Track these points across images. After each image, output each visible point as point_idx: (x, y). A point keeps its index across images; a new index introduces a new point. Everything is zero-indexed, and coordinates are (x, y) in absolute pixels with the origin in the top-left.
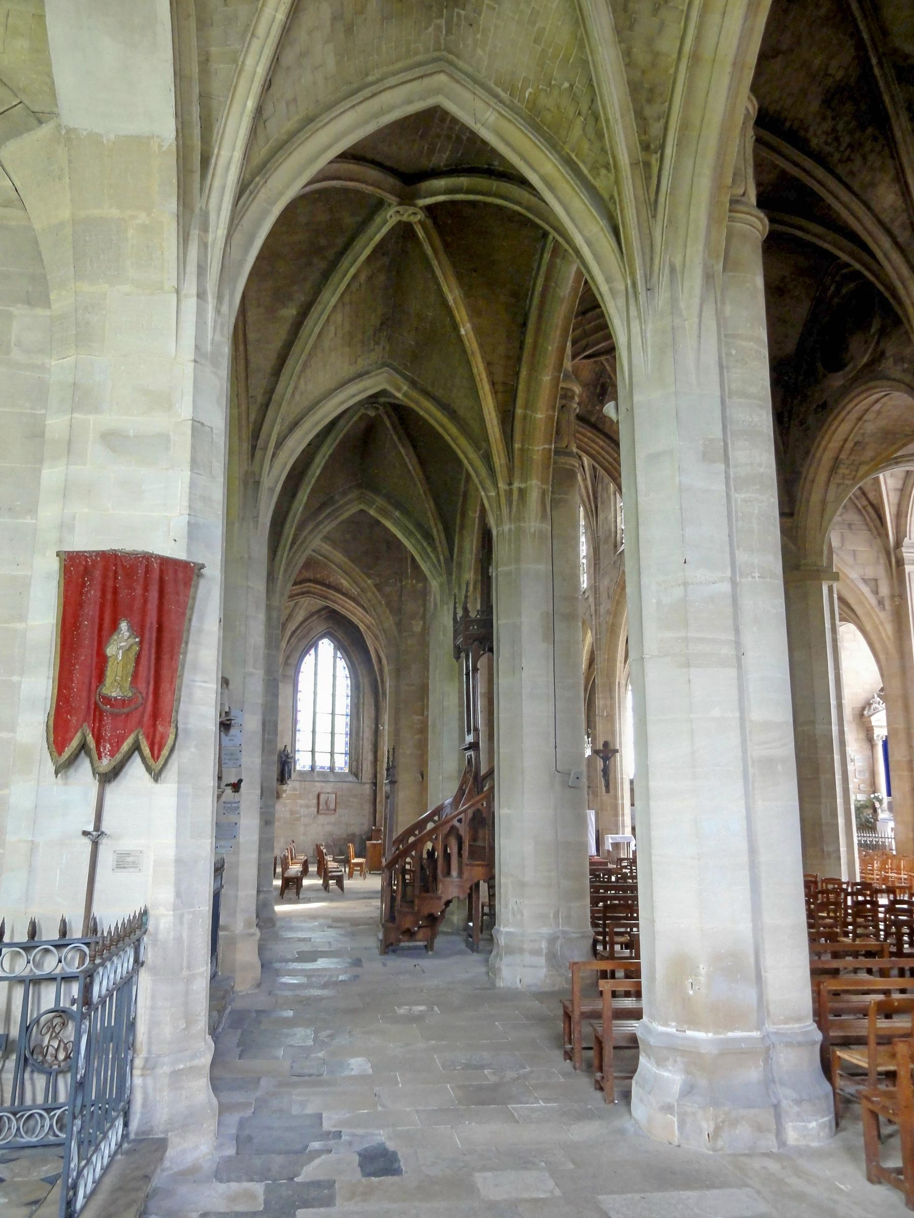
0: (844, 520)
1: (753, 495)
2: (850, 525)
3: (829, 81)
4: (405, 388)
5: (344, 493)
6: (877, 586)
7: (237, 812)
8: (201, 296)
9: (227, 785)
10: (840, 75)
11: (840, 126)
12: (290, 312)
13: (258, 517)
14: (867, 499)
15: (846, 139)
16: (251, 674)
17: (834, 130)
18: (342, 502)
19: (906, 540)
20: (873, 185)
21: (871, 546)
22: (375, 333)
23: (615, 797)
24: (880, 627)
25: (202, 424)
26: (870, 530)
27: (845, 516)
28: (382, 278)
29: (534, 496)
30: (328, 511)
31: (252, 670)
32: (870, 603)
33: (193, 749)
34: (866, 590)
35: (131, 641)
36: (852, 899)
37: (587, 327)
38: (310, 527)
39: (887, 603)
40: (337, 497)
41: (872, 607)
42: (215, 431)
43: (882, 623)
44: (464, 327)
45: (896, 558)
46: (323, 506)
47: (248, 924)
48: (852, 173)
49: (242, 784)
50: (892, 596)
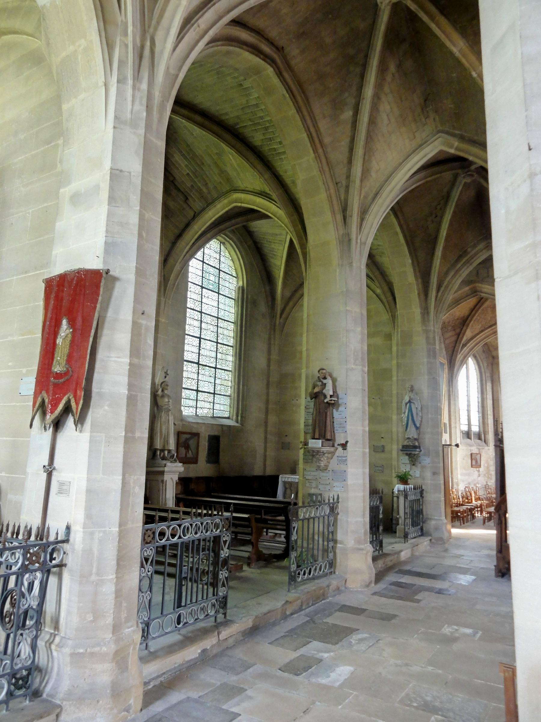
4: (456, 144)
5: (475, 246)
7: (345, 463)
8: (121, 81)
9: (338, 445)
12: (348, 114)
13: (352, 263)
16: (352, 369)
18: (473, 252)
22: (422, 109)
25: (121, 171)
28: (409, 64)
30: (464, 260)
31: (353, 366)
33: (106, 408)
35: (68, 331)
38: (452, 273)
40: (469, 250)
42: (132, 174)
44: (475, 70)
47: (358, 541)
49: (348, 444)
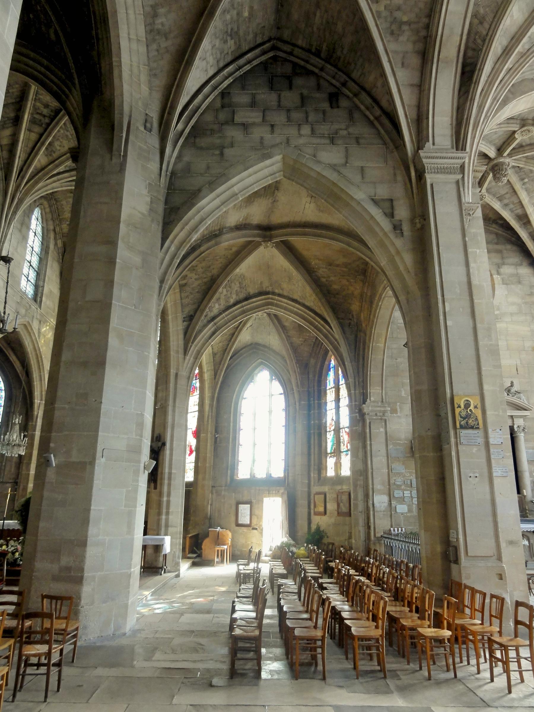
0: (349, 134)
2: (357, 140)
6: (392, 207)
14: (381, 108)
19: (429, 145)
21: (386, 161)
23: (161, 494)
24: (397, 259)
26: (385, 143)
27: (351, 130)
32: (382, 229)
34: (376, 213)
39: (406, 227)
41: (385, 234)
43: (398, 253)
45: (416, 171)
50: (412, 221)
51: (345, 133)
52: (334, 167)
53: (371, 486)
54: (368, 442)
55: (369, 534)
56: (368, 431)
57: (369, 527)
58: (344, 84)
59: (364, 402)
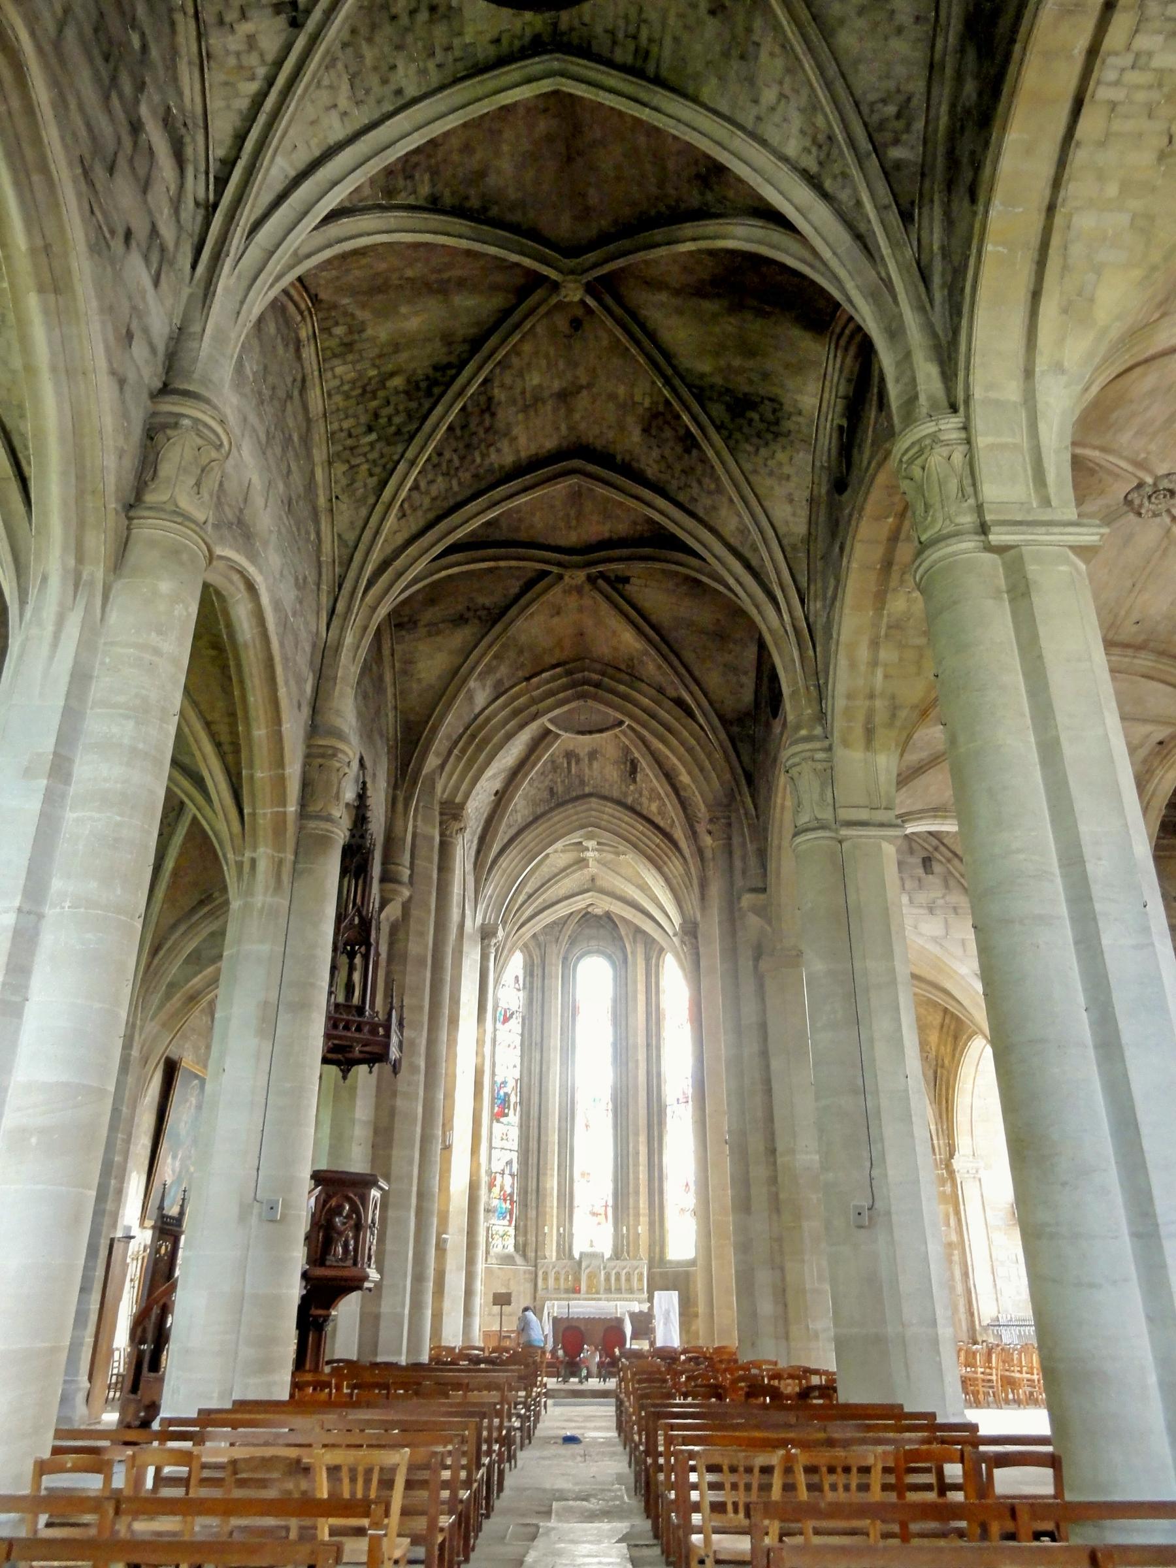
1: (88, 814)
2: (955, 909)
3: (640, 411)
10: (647, 403)
11: (667, 452)
15: (678, 468)
17: (663, 457)
20: (715, 508)
29: (262, 866)
30: (206, 910)
36: (815, 1398)
37: (534, 693)
38: (182, 928)
40: (216, 894)
46: (202, 903)
48: (694, 500)
51: (941, 902)
52: (935, 940)
53: (969, 1263)
54: (962, 1207)
55: (973, 1322)
56: (960, 1192)
57: (972, 1315)
58: (936, 849)
59: (952, 1156)
